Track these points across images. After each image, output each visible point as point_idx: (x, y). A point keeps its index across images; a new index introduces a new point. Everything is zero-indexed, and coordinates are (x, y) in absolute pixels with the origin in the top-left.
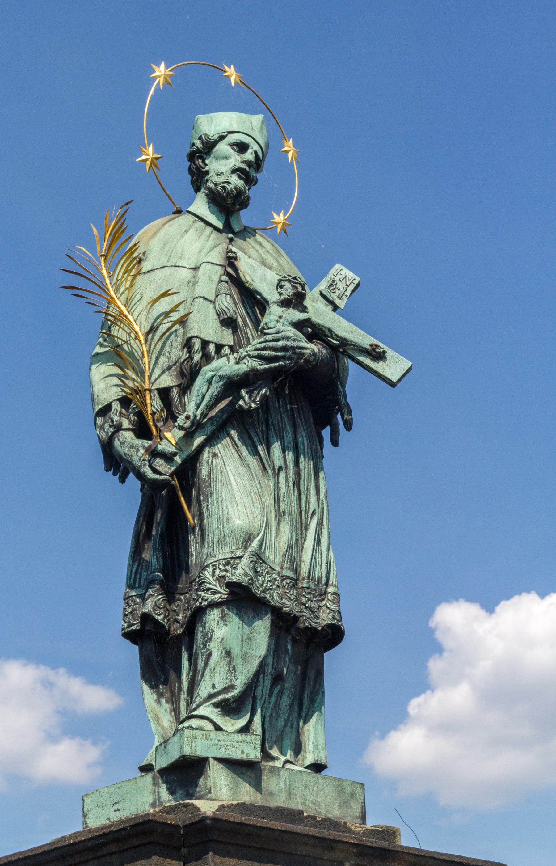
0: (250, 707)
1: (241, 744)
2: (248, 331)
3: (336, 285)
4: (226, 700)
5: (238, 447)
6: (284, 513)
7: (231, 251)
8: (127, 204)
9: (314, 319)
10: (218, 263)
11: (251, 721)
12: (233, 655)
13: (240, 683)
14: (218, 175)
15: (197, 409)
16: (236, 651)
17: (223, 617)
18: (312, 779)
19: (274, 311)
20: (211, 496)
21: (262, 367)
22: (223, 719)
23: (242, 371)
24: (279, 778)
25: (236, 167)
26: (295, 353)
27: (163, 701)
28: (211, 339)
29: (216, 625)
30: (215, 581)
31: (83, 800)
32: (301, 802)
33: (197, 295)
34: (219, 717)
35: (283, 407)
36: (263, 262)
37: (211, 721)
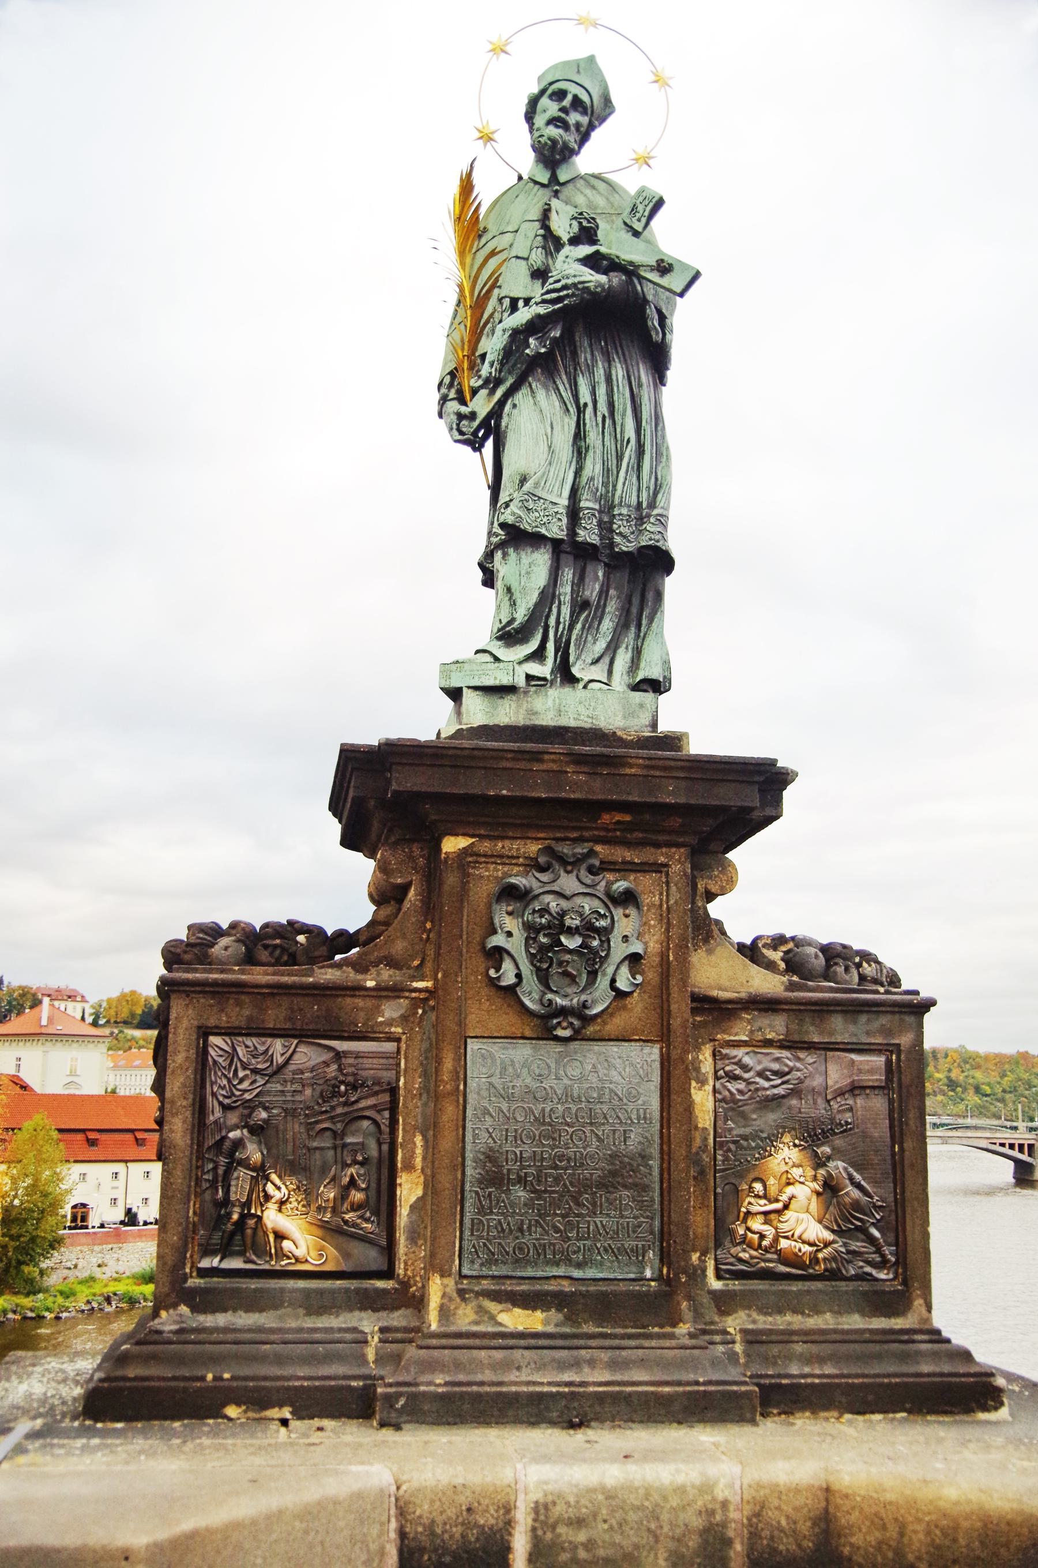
9: (603, 250)
12: (513, 590)
13: (521, 615)
15: (492, 366)
17: (505, 555)
19: (567, 250)
23: (524, 321)
26: (578, 289)
28: (520, 296)
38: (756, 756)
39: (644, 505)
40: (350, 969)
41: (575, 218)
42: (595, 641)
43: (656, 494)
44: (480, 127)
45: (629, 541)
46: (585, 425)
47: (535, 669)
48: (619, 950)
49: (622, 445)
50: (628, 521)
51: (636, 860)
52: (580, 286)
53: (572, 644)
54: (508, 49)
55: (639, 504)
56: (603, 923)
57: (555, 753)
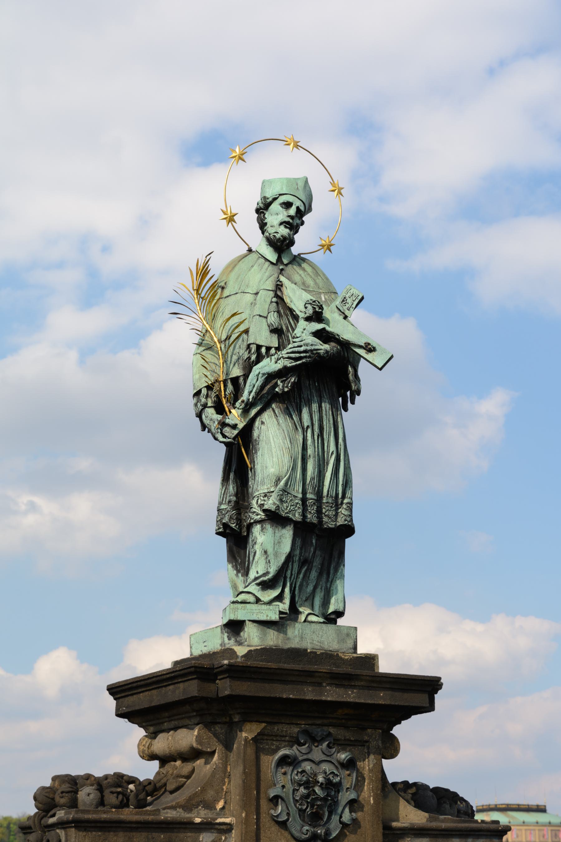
0: (282, 584)
1: (266, 611)
2: (290, 335)
3: (346, 300)
5: (277, 417)
6: (310, 456)
7: (279, 281)
8: (210, 254)
9: (328, 328)
10: (271, 289)
12: (268, 553)
13: (273, 571)
16: (270, 551)
17: (262, 529)
18: (318, 628)
19: (302, 323)
20: (259, 451)
21: (290, 365)
22: (263, 592)
23: (277, 369)
24: (295, 629)
25: (283, 221)
26: (313, 354)
27: (240, 575)
28: (263, 344)
29: (258, 534)
30: (258, 507)
31: (190, 638)
32: (310, 642)
33: (255, 314)
34: (259, 592)
35: (312, 384)
36: (304, 283)
37: (254, 595)
38: (430, 675)
39: (340, 496)
40: (181, 810)
41: (310, 304)
42: (308, 585)
43: (346, 486)
44: (225, 209)
45: (333, 521)
48: (345, 797)
50: (331, 507)
51: (352, 739)
53: (297, 588)
54: (244, 157)
55: (337, 495)
57: (322, 672)
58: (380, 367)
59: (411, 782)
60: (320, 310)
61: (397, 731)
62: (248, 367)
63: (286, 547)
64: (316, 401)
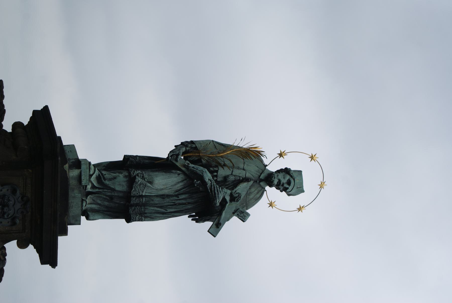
0: (100, 187)
3: (242, 213)
4: (101, 178)
5: (182, 181)
6: (164, 199)
7: (251, 180)
9: (228, 204)
10: (246, 176)
11: (96, 188)
13: (107, 182)
14: (278, 176)
15: (192, 167)
16: (116, 180)
19: (229, 192)
21: (208, 186)
23: (205, 180)
27: (104, 168)
28: (218, 173)
41: (239, 195)
42: (101, 200)
44: (285, 152)
46: (172, 197)
47: (89, 187)
49: (165, 208)
52: (215, 198)
53: (98, 195)
54: (313, 161)
55: (146, 213)
56: (6, 216)
58: (209, 231)
59: (6, 257)
60: (236, 200)
61: (31, 247)
62: (207, 166)
63: (118, 188)
64: (192, 201)
